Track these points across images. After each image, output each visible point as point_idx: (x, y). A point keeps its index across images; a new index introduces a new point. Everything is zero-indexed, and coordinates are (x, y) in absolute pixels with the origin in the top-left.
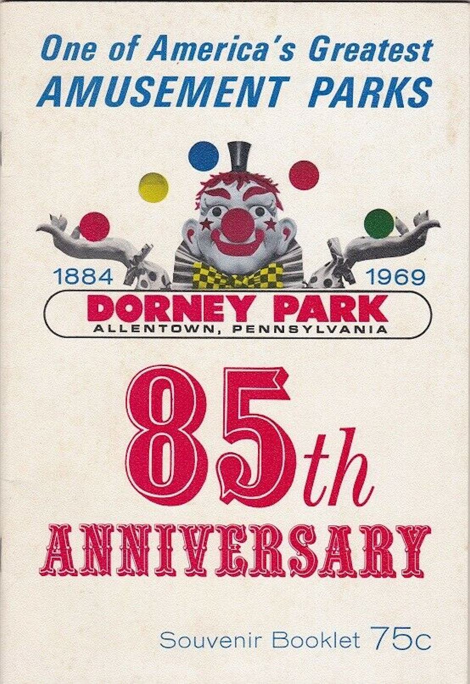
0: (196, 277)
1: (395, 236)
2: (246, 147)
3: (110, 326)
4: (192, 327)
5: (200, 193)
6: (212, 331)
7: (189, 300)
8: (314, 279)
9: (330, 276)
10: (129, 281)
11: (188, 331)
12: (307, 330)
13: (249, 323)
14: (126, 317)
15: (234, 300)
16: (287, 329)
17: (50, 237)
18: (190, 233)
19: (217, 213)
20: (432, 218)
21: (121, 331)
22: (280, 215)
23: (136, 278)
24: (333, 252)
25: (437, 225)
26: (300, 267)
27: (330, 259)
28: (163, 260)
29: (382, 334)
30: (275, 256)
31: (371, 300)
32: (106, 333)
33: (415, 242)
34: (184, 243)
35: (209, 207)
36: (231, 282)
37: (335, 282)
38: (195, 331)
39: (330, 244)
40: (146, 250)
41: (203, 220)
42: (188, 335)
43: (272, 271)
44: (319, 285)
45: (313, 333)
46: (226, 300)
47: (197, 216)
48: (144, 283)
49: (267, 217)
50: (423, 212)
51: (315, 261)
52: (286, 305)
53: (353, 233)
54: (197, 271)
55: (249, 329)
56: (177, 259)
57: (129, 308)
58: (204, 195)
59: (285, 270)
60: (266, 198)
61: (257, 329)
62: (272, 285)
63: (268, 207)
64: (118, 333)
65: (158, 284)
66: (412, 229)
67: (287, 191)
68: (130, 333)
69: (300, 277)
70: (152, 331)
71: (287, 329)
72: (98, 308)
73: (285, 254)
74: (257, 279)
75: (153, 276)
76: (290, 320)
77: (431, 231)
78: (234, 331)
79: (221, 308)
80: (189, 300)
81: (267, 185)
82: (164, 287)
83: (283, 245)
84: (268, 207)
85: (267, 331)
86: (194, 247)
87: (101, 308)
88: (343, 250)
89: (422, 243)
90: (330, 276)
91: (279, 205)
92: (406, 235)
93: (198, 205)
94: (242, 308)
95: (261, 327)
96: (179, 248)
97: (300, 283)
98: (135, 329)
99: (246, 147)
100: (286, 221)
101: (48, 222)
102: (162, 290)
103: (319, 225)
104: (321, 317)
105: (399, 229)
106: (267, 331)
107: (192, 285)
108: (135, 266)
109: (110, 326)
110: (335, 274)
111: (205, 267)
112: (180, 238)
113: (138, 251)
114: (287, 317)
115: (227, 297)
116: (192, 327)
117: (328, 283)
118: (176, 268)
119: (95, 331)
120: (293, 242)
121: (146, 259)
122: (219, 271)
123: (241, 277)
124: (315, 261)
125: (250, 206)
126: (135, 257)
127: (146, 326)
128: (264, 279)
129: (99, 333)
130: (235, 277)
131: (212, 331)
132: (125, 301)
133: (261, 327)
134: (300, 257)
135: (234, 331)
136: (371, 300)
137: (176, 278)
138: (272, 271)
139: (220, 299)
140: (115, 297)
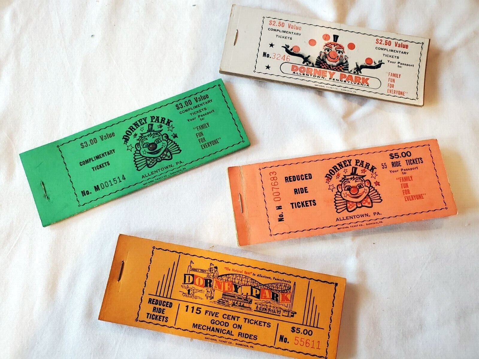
0: (321, 65)
1: (373, 65)
2: (338, 36)
3: (297, 73)
4: (319, 76)
5: (324, 46)
6: (324, 78)
7: (318, 70)
8: (351, 71)
9: (355, 71)
10: (303, 63)
11: (318, 77)
12: (349, 82)
13: (333, 78)
14: (301, 71)
15: (330, 73)
16: (343, 81)
17: (285, 49)
18: (320, 55)
19: (328, 51)
20: (383, 62)
21: (300, 74)
22: (344, 55)
23: (305, 63)
24: (357, 65)
25: (384, 63)
26: (348, 67)
27: (356, 67)
28: (314, 59)
29: (368, 87)
30: (342, 63)
31: (365, 79)
32: (296, 74)
33: (378, 66)
34: (319, 57)
35: (326, 49)
36: (330, 67)
37: (356, 72)
38: (319, 77)
39: (356, 63)
40: (309, 56)
41: (324, 51)
42: (318, 78)
43: (341, 67)
44: (352, 72)
45: (350, 83)
46: (328, 72)
47: (323, 51)
48: (307, 64)
49: (341, 53)
50: (381, 60)
51: (352, 67)
52: (343, 76)
53: (362, 62)
54: (322, 63)
55: (334, 79)
56: (317, 60)
57: (302, 70)
58: (325, 46)
59: (344, 67)
60: (341, 50)
61: (335, 80)
62: (341, 70)
63: (342, 52)
64: (299, 75)
65: (311, 65)
66: (378, 63)
67: (346, 49)
68: (302, 75)
69: (348, 70)
70: (308, 75)
71: (343, 81)
72: (294, 68)
73: (345, 63)
74: (337, 68)
75: (310, 63)
76: (344, 80)
77: (382, 65)
78: (330, 79)
79: (326, 74)
80: (318, 70)
81: (341, 47)
82: (312, 65)
83: (344, 61)
84: (342, 52)
85: (338, 81)
86: (321, 58)
87: (295, 68)
88: (359, 66)
89: (380, 67)
90: (355, 71)
91: (344, 52)
92: (376, 65)
93: (323, 49)
94: (332, 75)
95: (337, 80)
96: (318, 57)
97: (347, 71)
98: (304, 74)
99: (338, 36)
100: (346, 56)
101: (285, 46)
102: (311, 66)
103: (354, 59)
104: (352, 80)
105: (375, 64)
106: (338, 81)
107: (319, 66)
108: (306, 59)
109: (297, 73)
110: (356, 71)
111: (323, 63)
112: (318, 55)
113: (307, 56)
114: (343, 79)
115: (329, 72)
116: (319, 76)
117: (355, 72)
118: (316, 62)
119: (293, 73)
120: (347, 61)
121: (309, 58)
122: (327, 65)
123: (333, 66)
124: (352, 67)
125: (337, 51)
126: (306, 57)
127: (307, 75)
128: (339, 68)
129: (294, 74)
130: (331, 67)
131: (324, 78)
132: (301, 68)
133: (337, 80)
134: (348, 65)
135: (330, 79)
136: (365, 79)
137: (316, 64)
138: (341, 67)
139: (326, 72)
140: (299, 66)
